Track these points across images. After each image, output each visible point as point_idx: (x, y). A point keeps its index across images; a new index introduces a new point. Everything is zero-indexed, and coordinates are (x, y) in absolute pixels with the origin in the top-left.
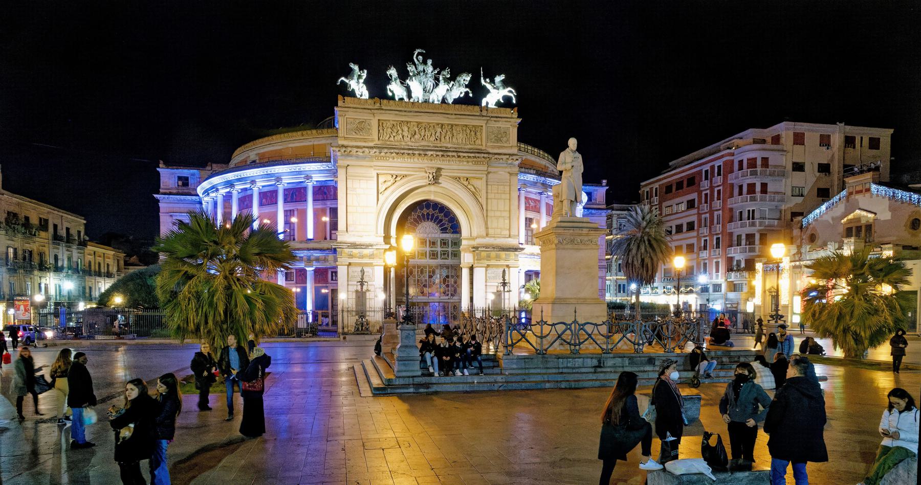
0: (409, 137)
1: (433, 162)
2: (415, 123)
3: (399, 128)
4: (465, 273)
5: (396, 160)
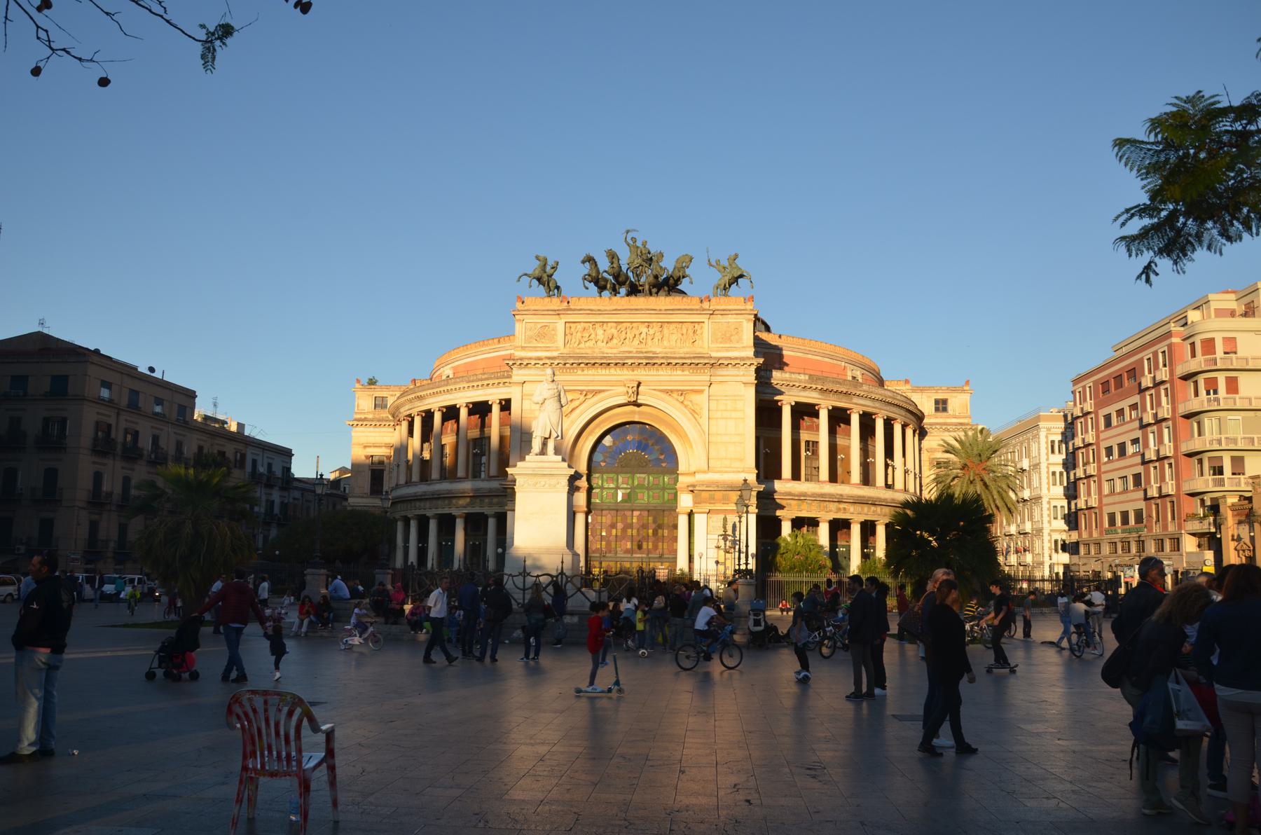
0: (605, 342)
1: (636, 372)
2: (612, 324)
3: (592, 331)
4: (683, 521)
5: (586, 372)
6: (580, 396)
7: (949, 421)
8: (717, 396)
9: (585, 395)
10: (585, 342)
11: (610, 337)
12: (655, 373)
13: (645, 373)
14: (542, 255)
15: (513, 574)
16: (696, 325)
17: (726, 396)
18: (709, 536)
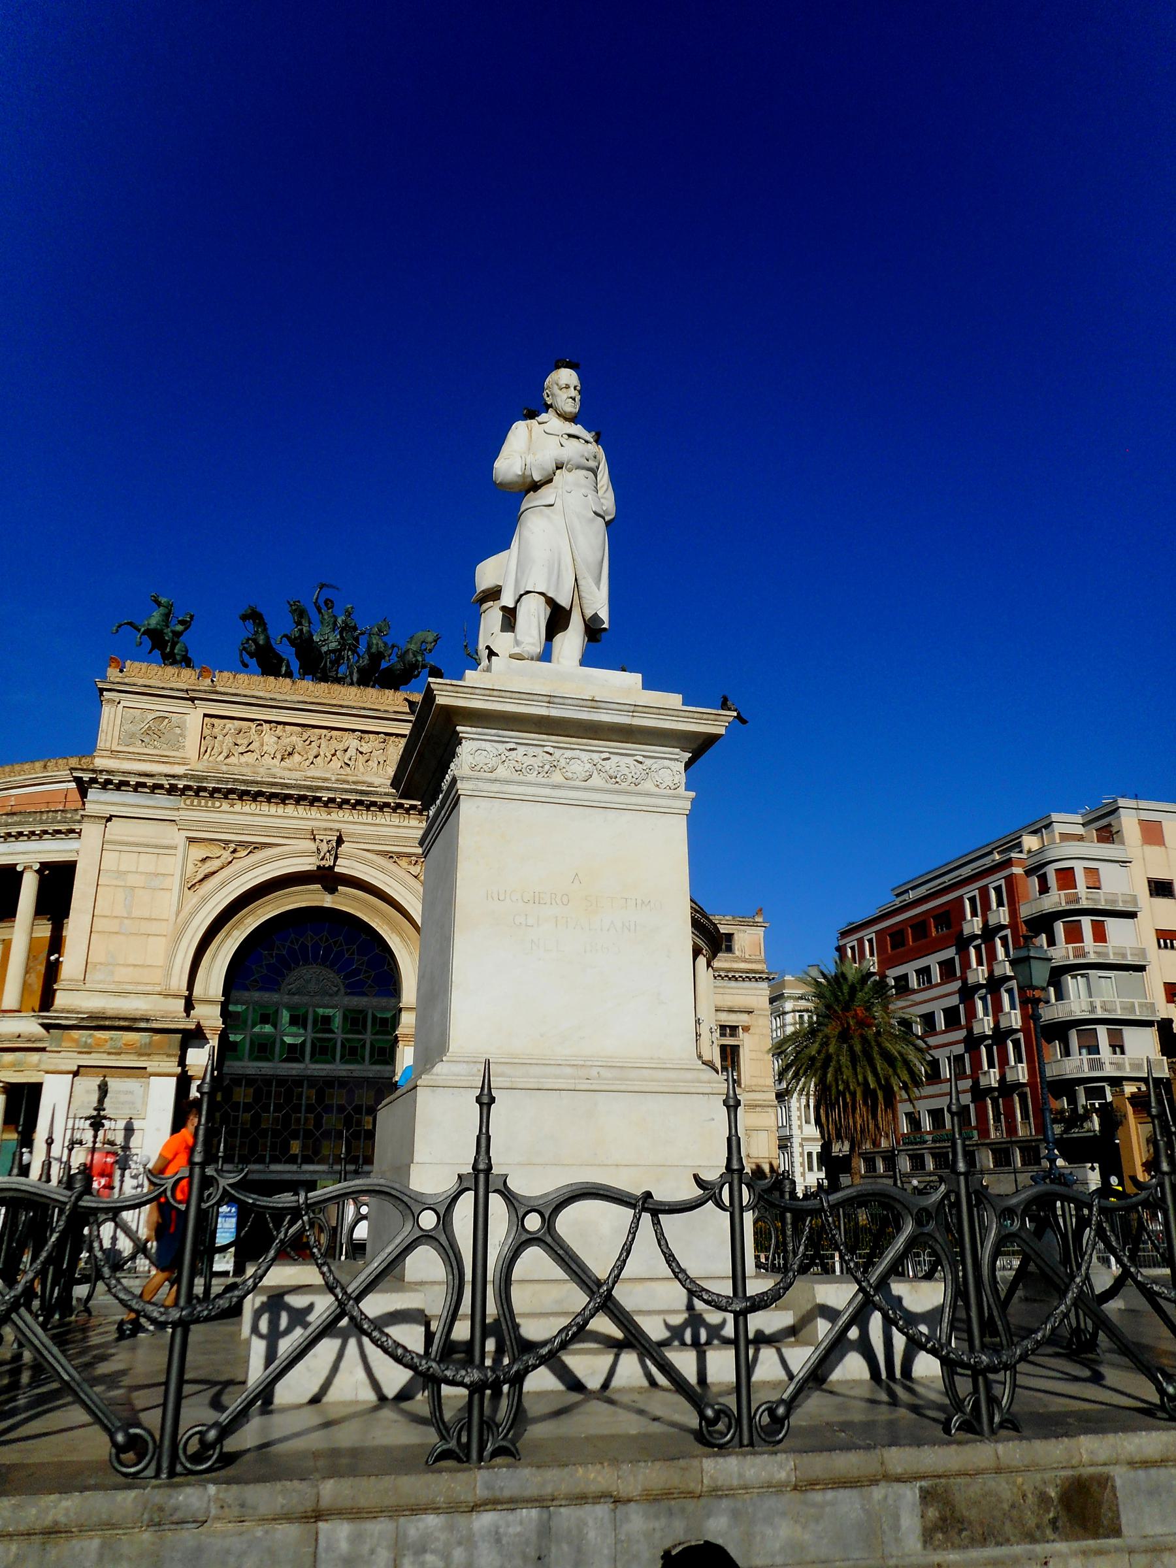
0: (279, 757)
1: (334, 816)
3: (255, 737)
6: (223, 852)
7: (735, 966)
9: (234, 851)
11: (290, 750)
12: (370, 820)
13: (351, 819)
15: (662, 1195)
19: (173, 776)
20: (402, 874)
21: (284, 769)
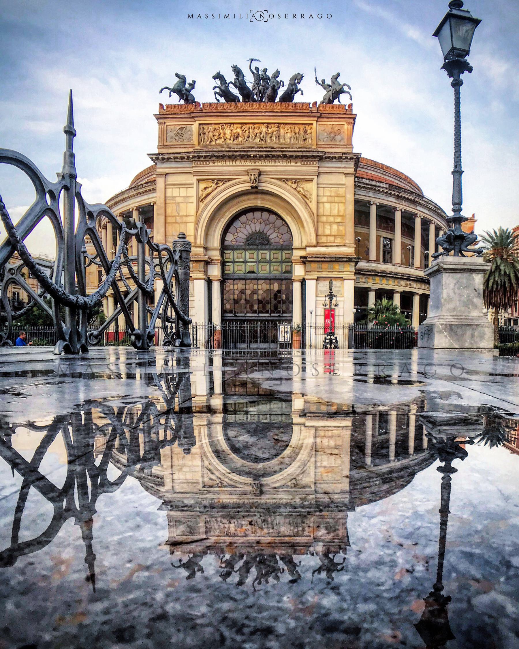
0: (232, 139)
1: (257, 164)
3: (221, 131)
5: (216, 164)
8: (323, 184)
10: (216, 140)
14: (181, 73)
16: (307, 126)
17: (331, 184)
18: (318, 299)
19: (187, 152)
20: (289, 188)
21: (235, 144)
